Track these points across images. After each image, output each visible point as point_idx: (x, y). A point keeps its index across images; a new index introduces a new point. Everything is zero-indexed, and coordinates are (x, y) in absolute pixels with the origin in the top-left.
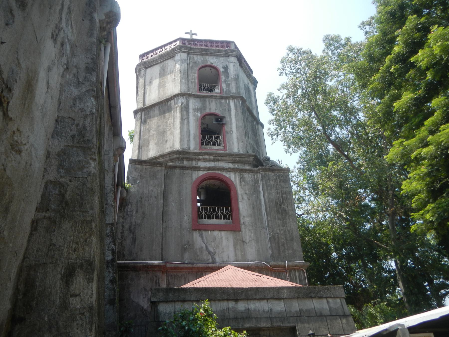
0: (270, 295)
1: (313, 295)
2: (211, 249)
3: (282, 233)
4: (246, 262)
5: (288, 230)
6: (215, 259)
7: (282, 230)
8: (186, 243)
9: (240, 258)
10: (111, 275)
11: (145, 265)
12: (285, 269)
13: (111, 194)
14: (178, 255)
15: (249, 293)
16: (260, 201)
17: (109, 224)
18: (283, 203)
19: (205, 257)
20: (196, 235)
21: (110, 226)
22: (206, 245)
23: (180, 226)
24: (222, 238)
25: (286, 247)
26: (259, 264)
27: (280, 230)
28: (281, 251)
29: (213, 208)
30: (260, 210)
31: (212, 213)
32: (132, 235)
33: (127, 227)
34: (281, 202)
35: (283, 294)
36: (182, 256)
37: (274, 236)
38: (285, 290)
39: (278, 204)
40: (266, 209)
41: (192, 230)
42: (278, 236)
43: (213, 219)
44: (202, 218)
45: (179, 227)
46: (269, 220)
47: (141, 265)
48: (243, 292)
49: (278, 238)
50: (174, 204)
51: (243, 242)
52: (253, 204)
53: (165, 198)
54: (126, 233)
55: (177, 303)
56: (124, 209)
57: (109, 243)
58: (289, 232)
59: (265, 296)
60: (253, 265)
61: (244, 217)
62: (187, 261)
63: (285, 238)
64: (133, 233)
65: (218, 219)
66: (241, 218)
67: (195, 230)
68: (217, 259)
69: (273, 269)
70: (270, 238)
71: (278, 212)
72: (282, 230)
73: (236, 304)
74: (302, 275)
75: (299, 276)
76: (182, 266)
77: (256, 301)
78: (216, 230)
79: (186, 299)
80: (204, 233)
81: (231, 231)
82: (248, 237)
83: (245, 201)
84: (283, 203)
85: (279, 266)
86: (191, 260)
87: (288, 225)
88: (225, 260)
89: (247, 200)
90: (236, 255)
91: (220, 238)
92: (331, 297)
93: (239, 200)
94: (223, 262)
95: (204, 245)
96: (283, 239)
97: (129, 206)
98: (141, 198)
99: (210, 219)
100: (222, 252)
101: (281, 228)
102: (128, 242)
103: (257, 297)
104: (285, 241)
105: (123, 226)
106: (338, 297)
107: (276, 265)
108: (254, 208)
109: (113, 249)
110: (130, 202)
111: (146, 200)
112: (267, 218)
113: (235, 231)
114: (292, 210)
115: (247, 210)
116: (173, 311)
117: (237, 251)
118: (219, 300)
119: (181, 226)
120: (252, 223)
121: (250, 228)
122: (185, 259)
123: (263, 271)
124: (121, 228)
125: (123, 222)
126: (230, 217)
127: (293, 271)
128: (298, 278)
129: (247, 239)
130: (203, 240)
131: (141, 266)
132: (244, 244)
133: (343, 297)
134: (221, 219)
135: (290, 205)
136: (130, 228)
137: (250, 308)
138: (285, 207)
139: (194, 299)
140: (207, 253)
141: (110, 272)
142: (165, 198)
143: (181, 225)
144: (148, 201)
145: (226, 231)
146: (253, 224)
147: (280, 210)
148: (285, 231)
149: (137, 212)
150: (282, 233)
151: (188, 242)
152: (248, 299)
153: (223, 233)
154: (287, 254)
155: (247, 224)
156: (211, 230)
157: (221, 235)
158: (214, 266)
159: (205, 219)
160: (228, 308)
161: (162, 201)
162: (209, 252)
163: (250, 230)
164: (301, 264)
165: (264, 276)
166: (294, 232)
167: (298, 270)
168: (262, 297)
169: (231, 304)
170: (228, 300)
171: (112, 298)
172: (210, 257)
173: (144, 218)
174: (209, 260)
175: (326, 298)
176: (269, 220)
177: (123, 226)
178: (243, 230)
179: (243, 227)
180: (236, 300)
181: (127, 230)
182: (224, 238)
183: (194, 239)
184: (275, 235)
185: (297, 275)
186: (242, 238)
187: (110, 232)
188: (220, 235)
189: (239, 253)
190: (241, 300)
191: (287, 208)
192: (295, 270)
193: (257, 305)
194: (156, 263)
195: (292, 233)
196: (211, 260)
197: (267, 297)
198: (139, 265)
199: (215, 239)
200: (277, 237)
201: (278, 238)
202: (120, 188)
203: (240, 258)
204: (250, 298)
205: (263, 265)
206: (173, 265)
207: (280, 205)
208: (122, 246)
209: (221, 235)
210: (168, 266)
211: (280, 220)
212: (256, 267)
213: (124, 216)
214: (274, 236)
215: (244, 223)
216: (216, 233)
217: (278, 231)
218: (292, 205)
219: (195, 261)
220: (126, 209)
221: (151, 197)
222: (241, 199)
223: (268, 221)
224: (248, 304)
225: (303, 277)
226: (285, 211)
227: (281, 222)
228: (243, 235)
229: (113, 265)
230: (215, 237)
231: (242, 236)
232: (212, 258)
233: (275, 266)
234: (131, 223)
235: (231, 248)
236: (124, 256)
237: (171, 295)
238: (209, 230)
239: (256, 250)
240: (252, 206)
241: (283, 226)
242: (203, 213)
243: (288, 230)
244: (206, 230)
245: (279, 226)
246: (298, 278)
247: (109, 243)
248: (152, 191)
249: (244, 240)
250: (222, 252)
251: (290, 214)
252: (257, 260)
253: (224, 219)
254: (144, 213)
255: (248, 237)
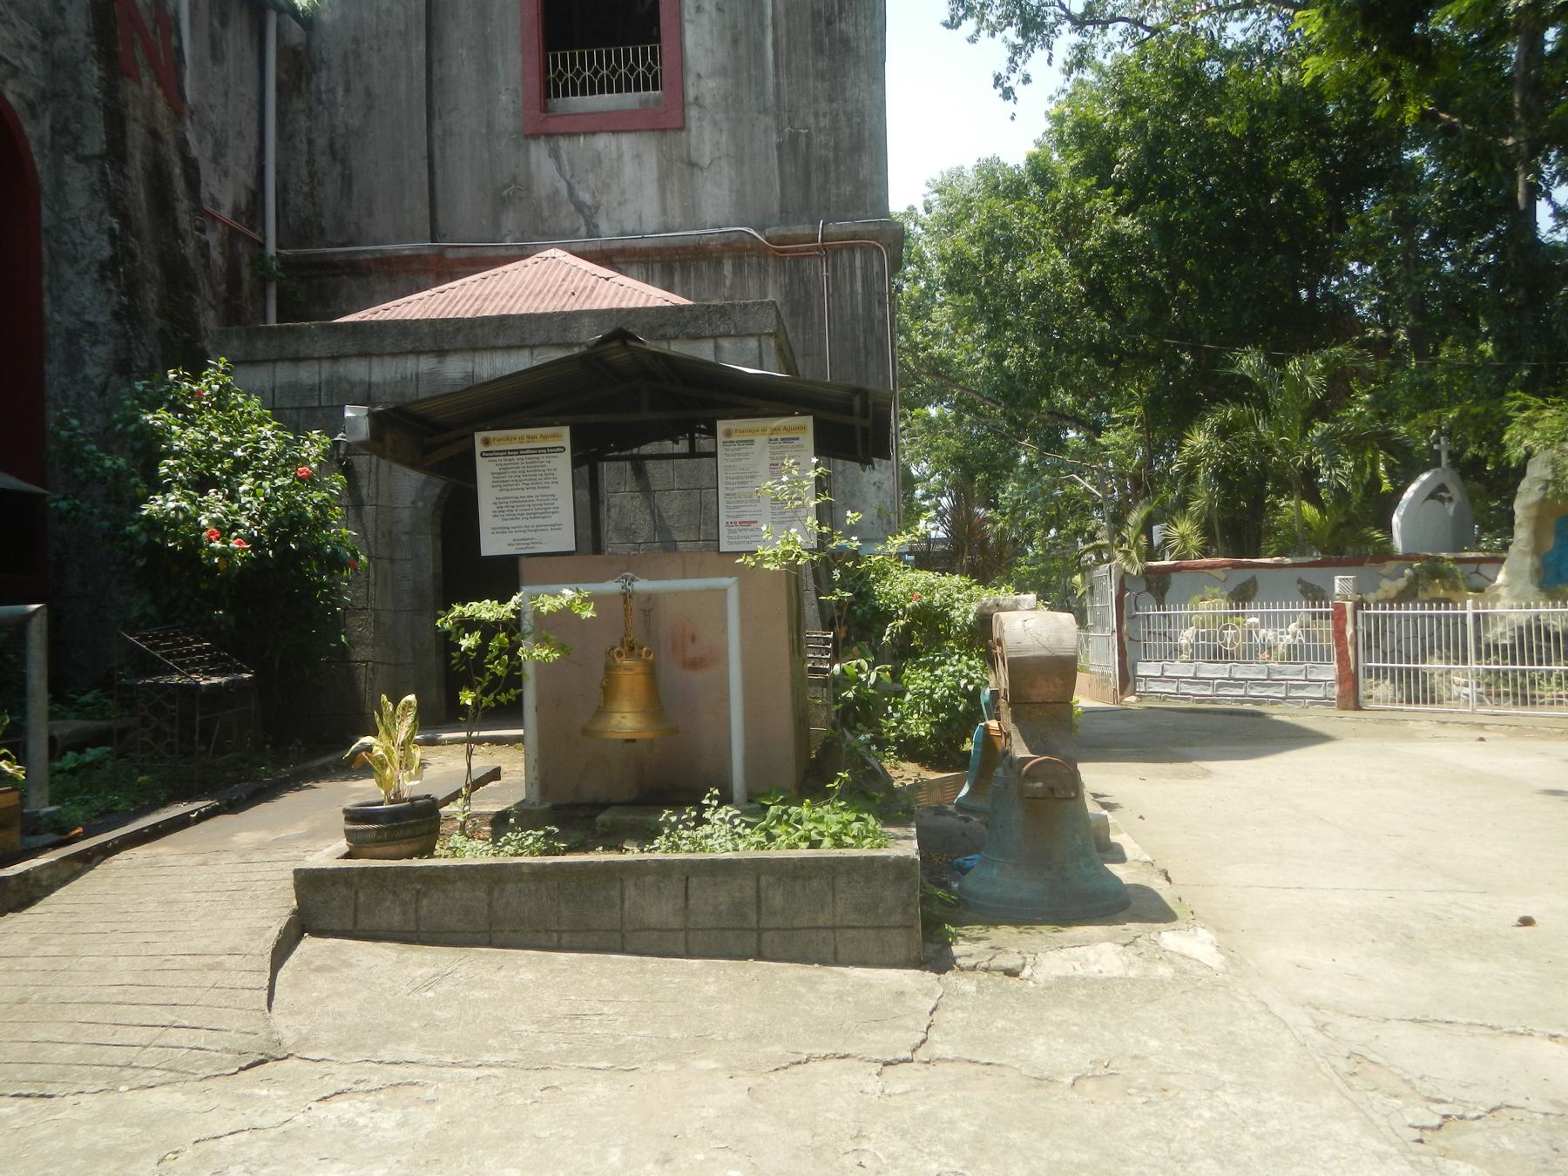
0: (540, 337)
1: (670, 331)
2: (585, 197)
3: (822, 124)
4: (695, 232)
5: (845, 113)
6: (597, 226)
7: (825, 116)
8: (506, 181)
9: (678, 221)
10: (115, 299)
11: (378, 255)
12: (818, 248)
13: (88, 64)
14: (484, 222)
15: (479, 331)
16: (762, 13)
17: (94, 157)
18: (840, 12)
19: (566, 224)
20: (539, 152)
21: (99, 162)
22: (569, 184)
23: (488, 127)
24: (620, 157)
25: (832, 175)
26: (734, 236)
27: (816, 115)
28: (814, 187)
29: (599, 54)
30: (758, 47)
31: (632, 70)
32: (338, 168)
33: (322, 142)
34: (833, 7)
35: (579, 331)
36: (496, 223)
37: (794, 139)
38: (586, 321)
39: (820, 17)
40: (775, 43)
41: (527, 136)
42: (808, 136)
43: (601, 92)
44: (566, 94)
45: (484, 130)
46: (784, 81)
47: (369, 256)
48: (458, 330)
49: (808, 145)
50: (463, 52)
51: (692, 165)
52: (734, 26)
53: (432, 36)
54: (323, 161)
55: (279, 365)
56: (309, 83)
57: (101, 213)
58: (849, 120)
59: (523, 339)
60: (712, 240)
61: (699, 76)
62: (508, 238)
63: (832, 143)
64: (343, 162)
65: (619, 91)
66: (690, 80)
67: (535, 136)
68: (604, 226)
69: (777, 250)
70: (780, 146)
71: (819, 48)
72: (825, 116)
73: (440, 362)
74: (876, 263)
75: (865, 268)
76: (491, 253)
77: (499, 353)
78: (601, 131)
79: (302, 355)
80: (564, 144)
81: (653, 130)
82: (707, 149)
83: (705, 19)
84: (840, 12)
85: (796, 240)
86: (522, 233)
87: (848, 94)
88: (629, 229)
89: (714, 13)
90: (664, 211)
91: (614, 156)
92: (727, 335)
93: (687, 16)
94: (623, 234)
95: (562, 186)
96: (826, 146)
97: (324, 74)
98: (356, 41)
99: (592, 93)
100: (620, 204)
101: (824, 106)
102: (330, 191)
103: (500, 342)
104: (831, 154)
105: (310, 142)
106: (751, 335)
107: (784, 236)
108: (735, 42)
109: (112, 230)
110: (322, 60)
111: (371, 48)
112: (777, 75)
113: (664, 130)
114: (873, 37)
115: (712, 52)
116: (268, 385)
117: (669, 195)
118: (394, 355)
119: (490, 126)
120: (725, 98)
121: (720, 117)
122: (504, 231)
123: (749, 256)
124: (304, 146)
125: (309, 129)
126: (652, 81)
127: (845, 253)
128: (859, 272)
129: (705, 154)
130: (560, 170)
131: (366, 260)
132: (692, 174)
133: (770, 335)
134: (628, 90)
135: (865, 17)
136: (332, 144)
137: (477, 371)
138: (845, 26)
139: (324, 354)
140: (573, 208)
141: (109, 291)
142: (432, 36)
143: (489, 122)
144: (380, 49)
145: (635, 131)
146: (730, 101)
147: (827, 40)
148: (835, 119)
149: (347, 90)
150: (822, 124)
151: (514, 179)
152: (474, 348)
153: (627, 142)
154: (833, 199)
155: (708, 101)
156: (585, 134)
157: (619, 148)
158: (587, 248)
159: (574, 94)
160: (417, 375)
161: (422, 47)
162: (580, 207)
163: (715, 123)
164: (871, 227)
165: (621, 279)
166: (867, 119)
167: (862, 247)
168: (514, 342)
169: (426, 364)
170: (417, 352)
171: (123, 356)
172: (582, 221)
173: (370, 108)
174: (578, 229)
175: (714, 337)
176: (784, 81)
177: (310, 142)
178: (693, 124)
179: (693, 112)
180: (441, 353)
181: (324, 153)
182: (627, 157)
183: (533, 167)
184: (798, 134)
185: (858, 263)
186: (689, 151)
187: (101, 181)
188: (613, 148)
189: (675, 204)
190: (456, 351)
191: (852, 29)
192: (852, 248)
193: (498, 365)
194: (406, 248)
195: (859, 124)
196: (583, 230)
197: (527, 342)
198: (361, 257)
199: (597, 160)
200: (803, 140)
201: (808, 145)
202: (272, 19)
203: (678, 221)
204: (480, 344)
205: (745, 236)
206: (464, 253)
207: (829, 23)
208: (314, 204)
209: (619, 148)
210: (450, 254)
211: (823, 79)
212: (723, 245)
213: (311, 109)
214: (794, 139)
215: (696, 99)
216: (602, 142)
217: (811, 120)
218: (873, 16)
219: (534, 237)
220: (313, 85)
221: (387, 34)
222: (693, 10)
223: (778, 86)
224: (474, 362)
225: (876, 268)
226: (845, 41)
227: (826, 84)
228: (693, 141)
229: (116, 273)
230: (599, 156)
231: (689, 146)
232: (588, 223)
233: (782, 240)
234: (333, 127)
235: (651, 190)
236: (322, 232)
237: (260, 344)
238: (578, 134)
239: (731, 191)
240: (729, 37)
241: (831, 100)
242: (569, 75)
243: (845, 113)
244: (570, 135)
245: (816, 100)
246: (859, 272)
247: (101, 213)
248: (389, 12)
249: (694, 157)
250: (620, 204)
251: (862, 53)
252: (732, 222)
253: (637, 89)
254: (368, 93)
255: (707, 149)
